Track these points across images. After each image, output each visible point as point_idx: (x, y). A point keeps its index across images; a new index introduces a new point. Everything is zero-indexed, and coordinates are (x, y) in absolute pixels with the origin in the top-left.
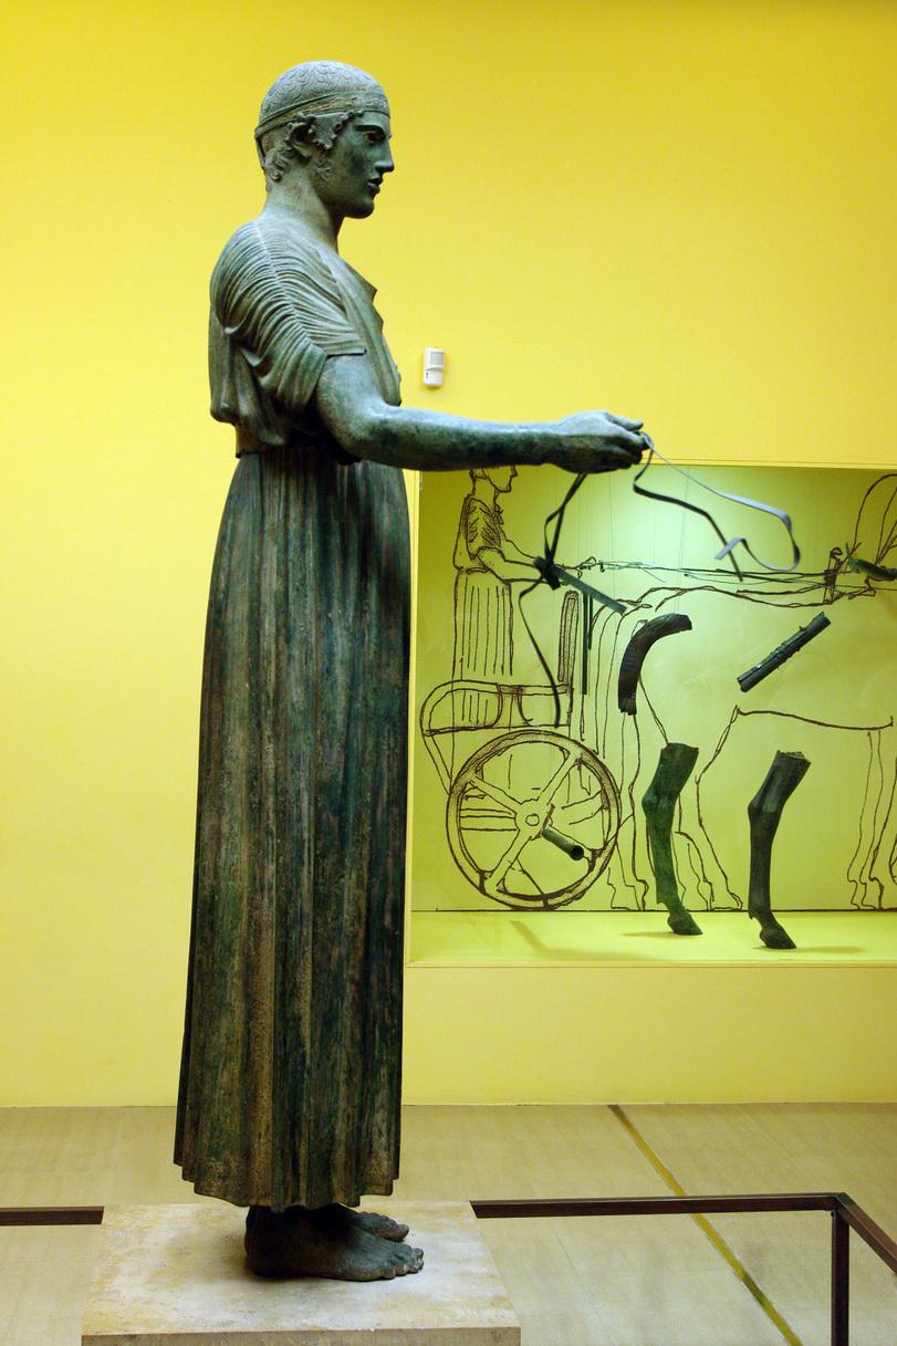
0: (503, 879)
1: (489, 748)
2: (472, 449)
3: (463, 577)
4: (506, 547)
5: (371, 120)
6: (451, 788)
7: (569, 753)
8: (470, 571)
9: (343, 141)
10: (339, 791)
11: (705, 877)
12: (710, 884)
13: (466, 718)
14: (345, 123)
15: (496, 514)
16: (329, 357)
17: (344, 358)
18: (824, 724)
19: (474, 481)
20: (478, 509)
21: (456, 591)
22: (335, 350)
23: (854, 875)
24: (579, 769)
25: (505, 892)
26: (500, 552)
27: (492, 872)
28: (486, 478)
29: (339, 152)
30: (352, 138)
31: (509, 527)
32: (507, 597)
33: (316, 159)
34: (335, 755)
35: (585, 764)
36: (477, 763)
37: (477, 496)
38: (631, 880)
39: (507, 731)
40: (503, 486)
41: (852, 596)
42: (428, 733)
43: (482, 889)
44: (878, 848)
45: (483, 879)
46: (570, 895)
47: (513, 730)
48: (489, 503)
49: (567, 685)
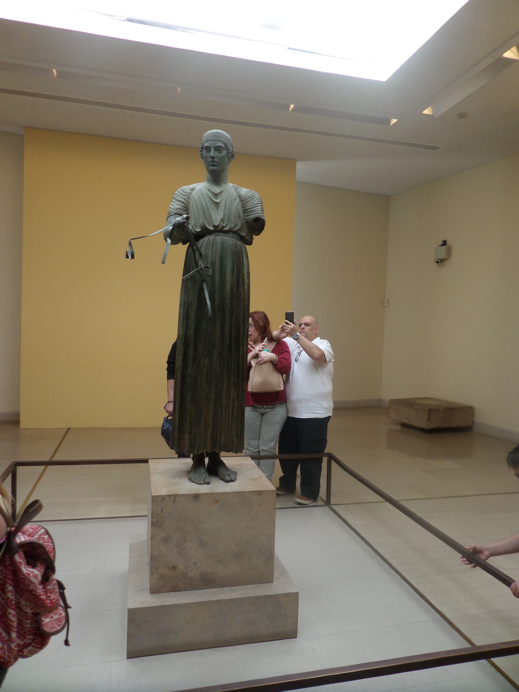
5: (205, 145)
30: (204, 152)
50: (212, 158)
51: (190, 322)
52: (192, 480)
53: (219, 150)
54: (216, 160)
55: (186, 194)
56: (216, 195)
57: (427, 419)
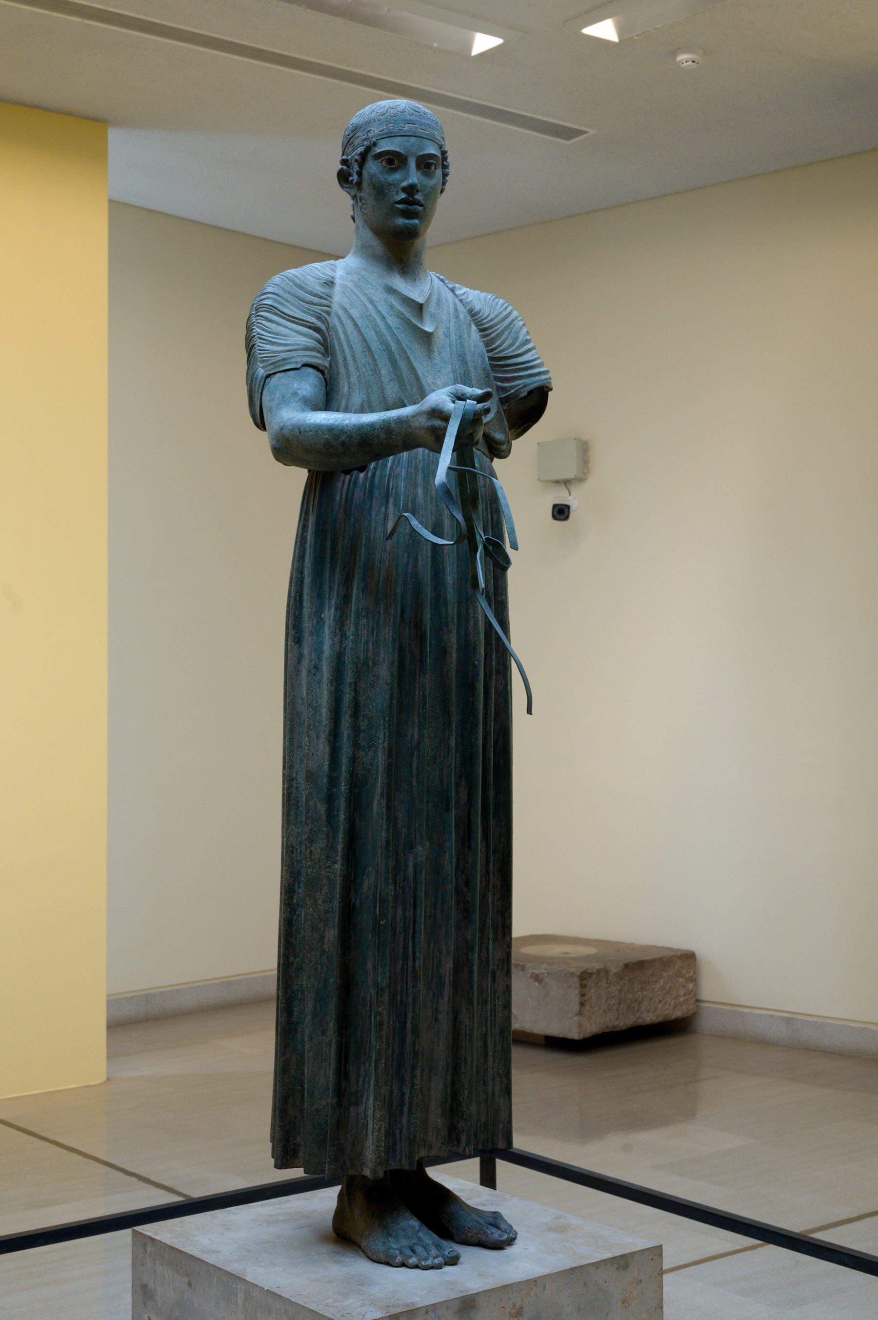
2: (343, 444)
5: (385, 146)
9: (365, 173)
10: (325, 780)
14: (364, 156)
16: (268, 376)
17: (278, 375)
22: (270, 370)
29: (365, 184)
30: (373, 167)
33: (358, 195)
34: (321, 747)
50: (411, 190)
51: (363, 725)
52: (399, 1259)
53: (428, 166)
54: (418, 197)
55: (316, 300)
56: (419, 309)
57: (576, 1007)
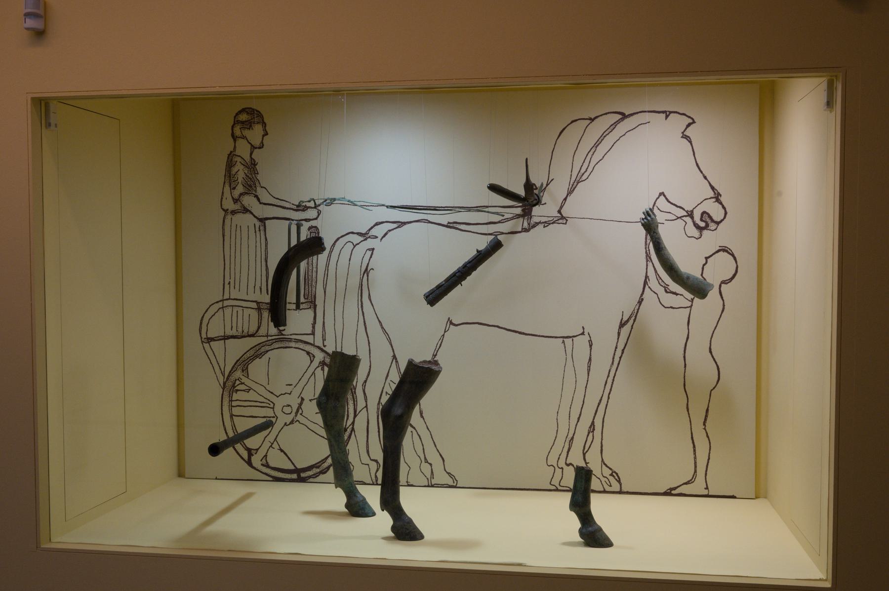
0: (266, 456)
1: (252, 352)
3: (229, 217)
4: (260, 192)
6: (224, 384)
7: (314, 357)
8: (234, 212)
11: (425, 459)
12: (431, 464)
13: (234, 328)
15: (252, 166)
18: (524, 334)
19: (235, 141)
20: (238, 163)
21: (223, 229)
23: (553, 460)
24: (323, 369)
25: (267, 465)
26: (256, 196)
27: (257, 450)
28: (244, 137)
31: (263, 177)
32: (262, 233)
35: (327, 365)
36: (243, 364)
37: (237, 153)
38: (366, 459)
39: (265, 339)
40: (257, 143)
41: (546, 224)
42: (206, 341)
43: (249, 463)
44: (572, 438)
45: (250, 455)
46: (318, 470)
47: (270, 338)
48: (247, 158)
49: (311, 302)
